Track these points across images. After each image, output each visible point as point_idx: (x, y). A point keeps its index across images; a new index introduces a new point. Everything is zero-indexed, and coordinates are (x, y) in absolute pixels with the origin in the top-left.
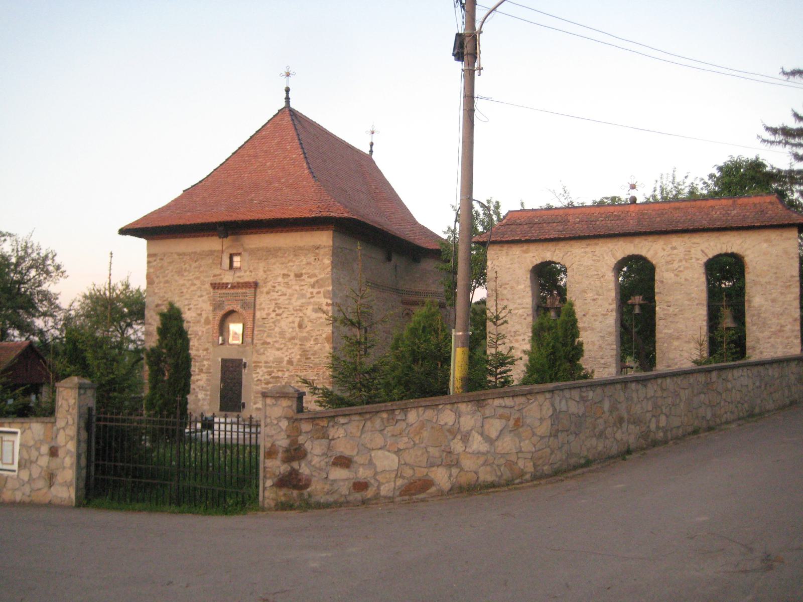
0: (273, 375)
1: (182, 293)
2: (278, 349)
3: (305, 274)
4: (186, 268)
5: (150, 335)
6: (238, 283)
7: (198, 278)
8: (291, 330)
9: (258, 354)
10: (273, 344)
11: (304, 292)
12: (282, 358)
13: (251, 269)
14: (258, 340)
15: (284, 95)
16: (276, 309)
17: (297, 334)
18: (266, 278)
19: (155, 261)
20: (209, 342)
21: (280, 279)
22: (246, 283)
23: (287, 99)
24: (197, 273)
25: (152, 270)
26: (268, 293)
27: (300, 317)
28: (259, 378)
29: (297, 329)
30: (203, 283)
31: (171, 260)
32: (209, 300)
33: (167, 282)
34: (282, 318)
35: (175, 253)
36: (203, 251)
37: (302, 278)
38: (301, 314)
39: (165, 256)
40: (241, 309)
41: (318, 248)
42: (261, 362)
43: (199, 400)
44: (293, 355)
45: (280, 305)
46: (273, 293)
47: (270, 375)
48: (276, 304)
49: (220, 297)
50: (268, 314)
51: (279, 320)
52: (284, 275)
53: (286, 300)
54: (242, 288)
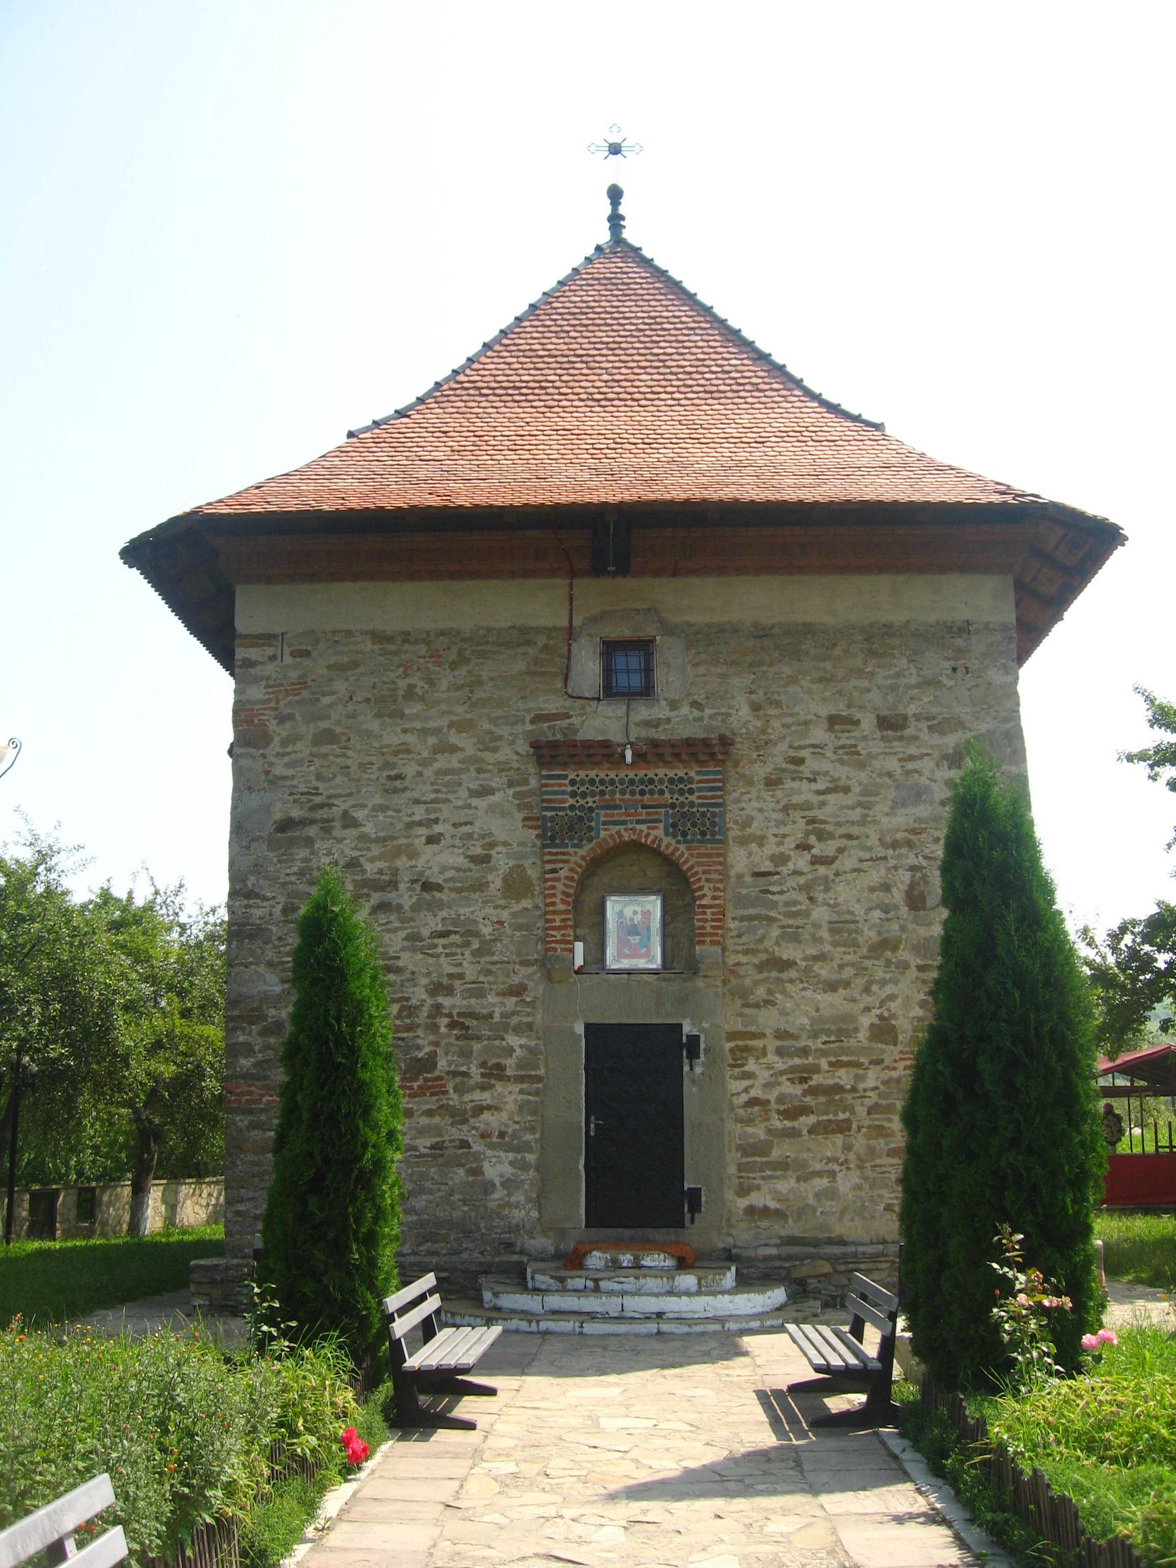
0: (816, 1079)
1: (399, 777)
2: (832, 987)
3: (918, 717)
4: (411, 687)
5: (252, 937)
6: (654, 743)
7: (462, 726)
8: (877, 914)
9: (746, 1005)
10: (807, 969)
11: (924, 780)
12: (851, 1018)
13: (700, 698)
14: (746, 952)
15: (608, 210)
16: (812, 839)
17: (903, 929)
18: (764, 731)
19: (273, 658)
20: (526, 963)
21: (819, 734)
22: (689, 742)
23: (616, 221)
24: (459, 709)
25: (257, 693)
26: (772, 783)
27: (912, 868)
28: (753, 1093)
29: (904, 910)
30: (490, 743)
31: (346, 659)
32: (520, 808)
33: (328, 737)
34: (837, 874)
35: (364, 633)
36: (489, 630)
37: (907, 732)
38: (912, 860)
39: (316, 641)
40: (666, 840)
41: (964, 629)
42: (763, 1035)
43: (488, 1187)
44: (893, 1005)
45: (829, 828)
46: (796, 784)
47: (803, 1080)
48: (812, 821)
49: (573, 794)
50: (780, 859)
51: (826, 878)
52: (834, 721)
53: (853, 808)
54: (667, 764)
